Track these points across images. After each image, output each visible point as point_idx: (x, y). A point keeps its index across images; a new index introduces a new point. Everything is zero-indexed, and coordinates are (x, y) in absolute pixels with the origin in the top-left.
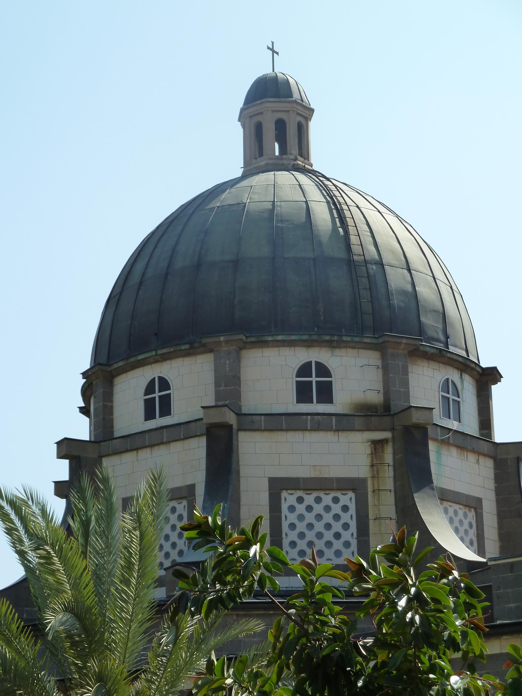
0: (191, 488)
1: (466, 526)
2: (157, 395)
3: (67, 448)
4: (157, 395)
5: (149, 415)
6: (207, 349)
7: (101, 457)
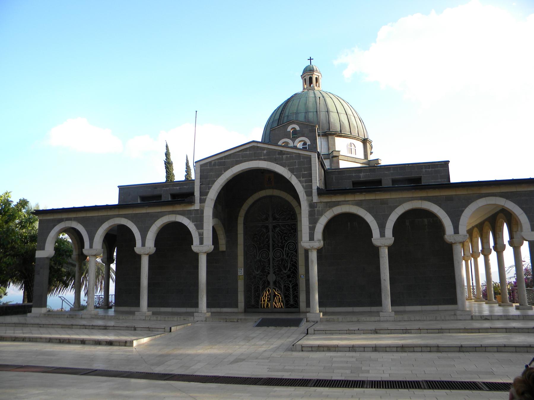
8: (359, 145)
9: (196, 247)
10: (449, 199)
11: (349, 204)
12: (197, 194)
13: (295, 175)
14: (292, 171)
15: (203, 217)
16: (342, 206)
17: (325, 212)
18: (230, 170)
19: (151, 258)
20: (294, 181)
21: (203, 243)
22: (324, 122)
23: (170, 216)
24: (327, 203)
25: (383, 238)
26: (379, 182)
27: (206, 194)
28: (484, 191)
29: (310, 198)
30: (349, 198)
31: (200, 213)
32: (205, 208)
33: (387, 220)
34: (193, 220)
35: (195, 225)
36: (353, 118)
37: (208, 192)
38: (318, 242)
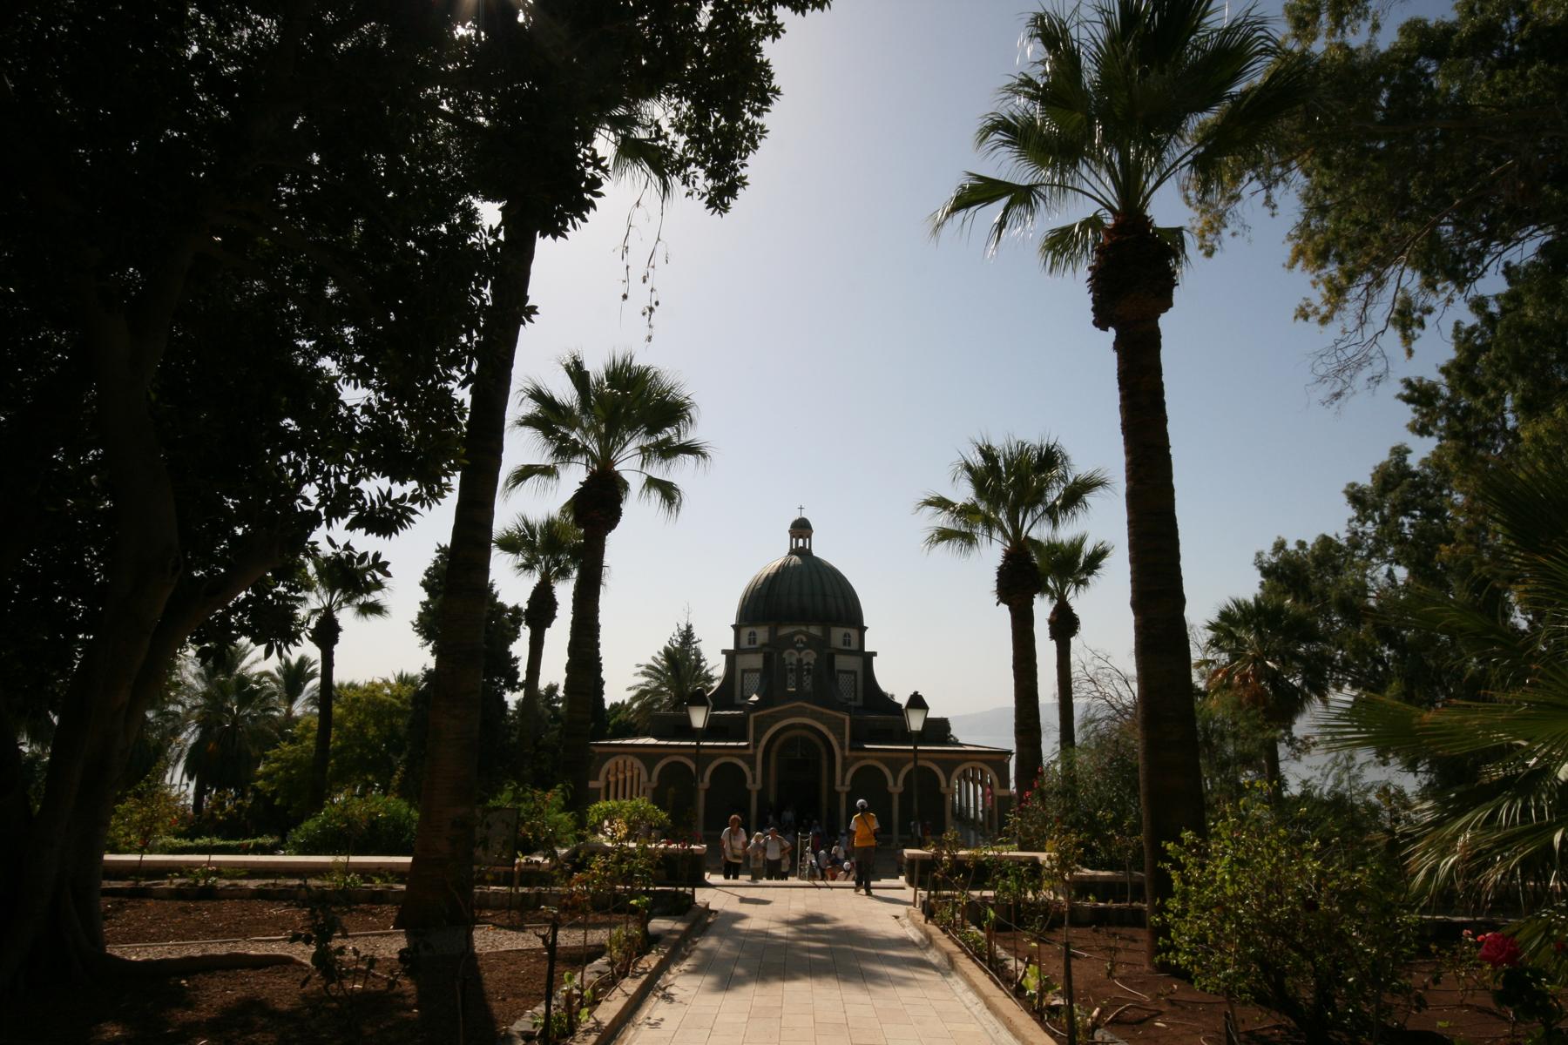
3: (724, 652)
14: (830, 728)
20: (832, 738)
21: (754, 784)
31: (754, 756)
34: (748, 763)
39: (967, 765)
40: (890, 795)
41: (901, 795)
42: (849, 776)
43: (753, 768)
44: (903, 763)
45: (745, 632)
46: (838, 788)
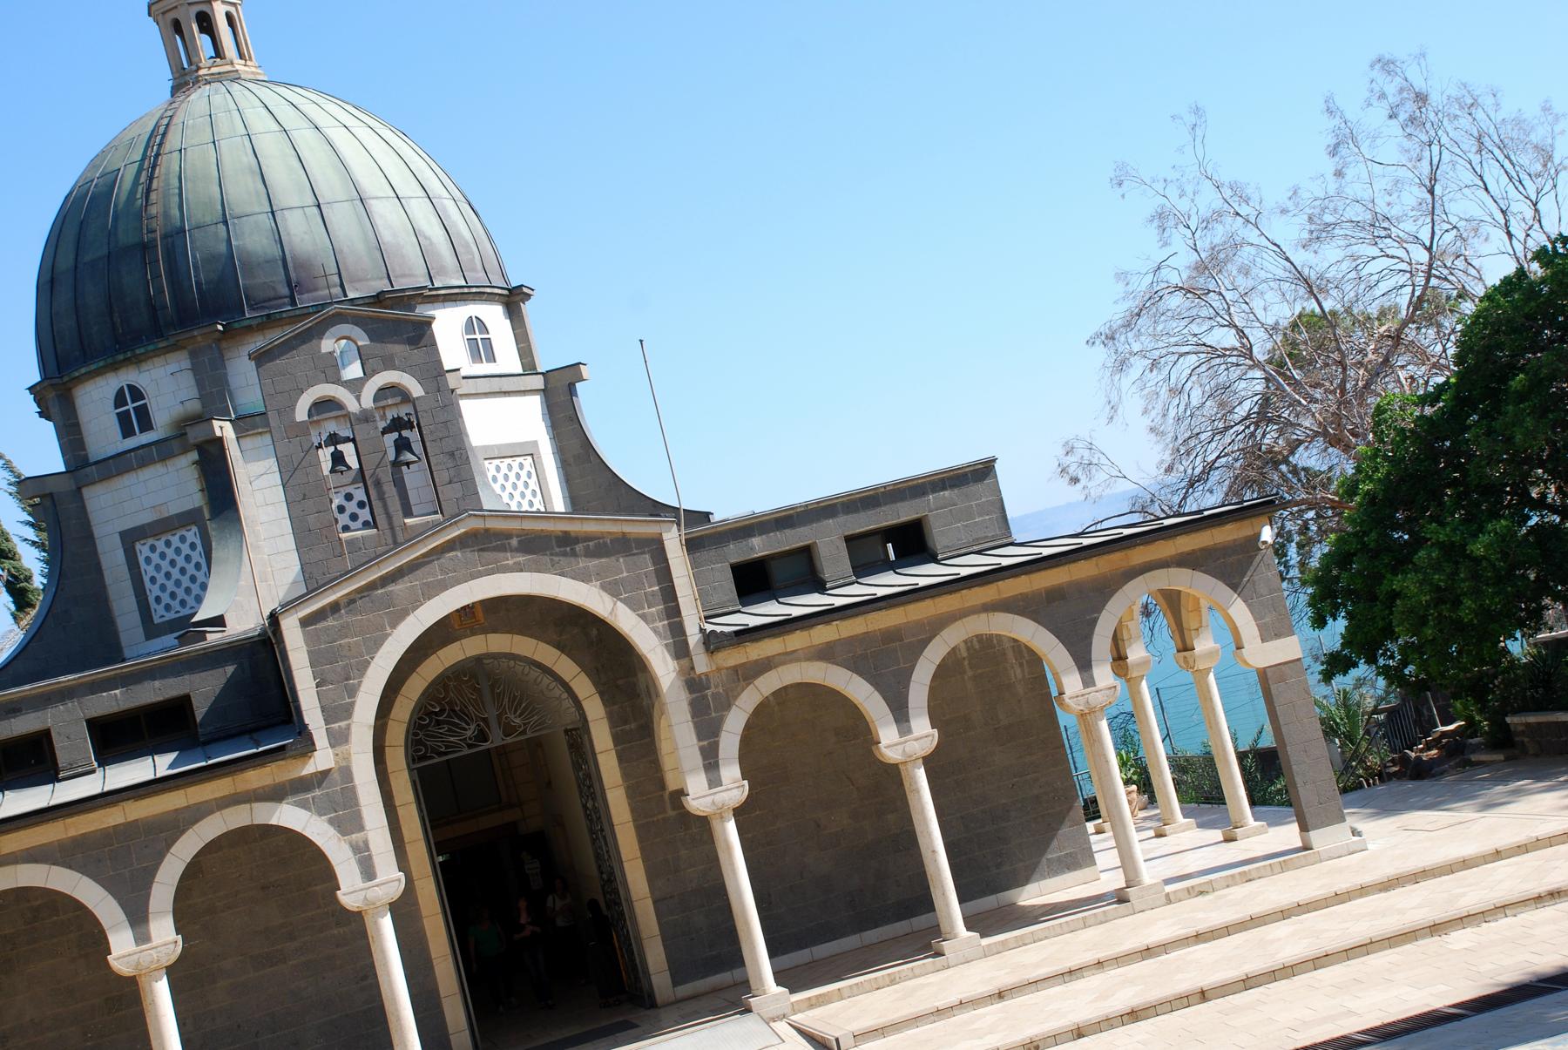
0: (199, 510)
1: (524, 477)
2: (130, 406)
4: (130, 406)
5: (127, 432)
6: (175, 348)
7: (79, 489)
8: (493, 315)
9: (351, 891)
10: (1055, 595)
11: (798, 660)
12: (313, 716)
13: (624, 601)
14: (612, 589)
15: (354, 787)
16: (780, 669)
17: (736, 697)
18: (410, 619)
19: (176, 974)
22: (360, 247)
23: (226, 812)
24: (735, 669)
25: (906, 741)
26: (806, 554)
27: (347, 711)
28: (1139, 555)
29: (685, 661)
30: (797, 640)
32: (354, 758)
33: (907, 687)
35: (331, 822)
36: (450, 205)
37: (352, 704)
38: (733, 787)
39: (1137, 593)
40: (892, 775)
41: (931, 763)
42: (730, 742)
43: (348, 822)
44: (910, 644)
45: (96, 400)
46: (700, 796)
